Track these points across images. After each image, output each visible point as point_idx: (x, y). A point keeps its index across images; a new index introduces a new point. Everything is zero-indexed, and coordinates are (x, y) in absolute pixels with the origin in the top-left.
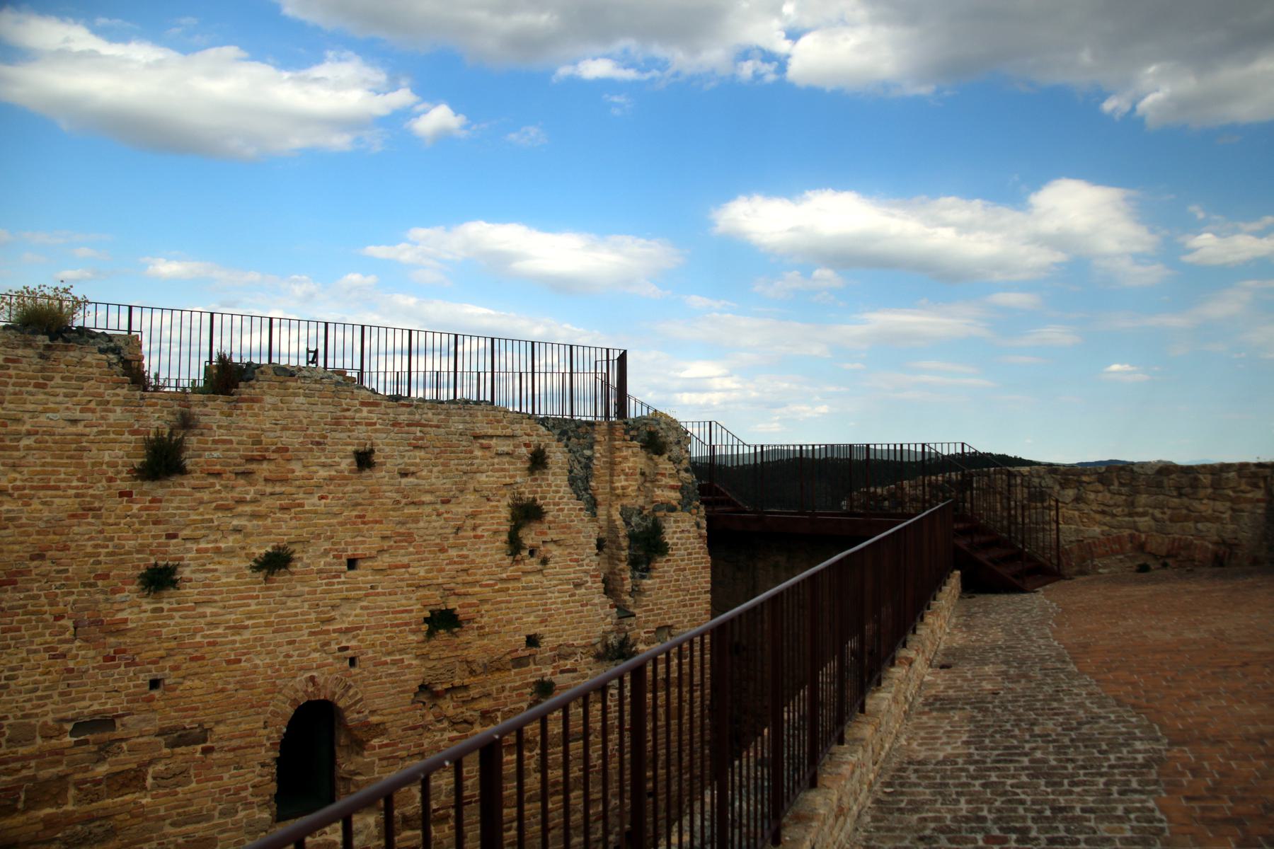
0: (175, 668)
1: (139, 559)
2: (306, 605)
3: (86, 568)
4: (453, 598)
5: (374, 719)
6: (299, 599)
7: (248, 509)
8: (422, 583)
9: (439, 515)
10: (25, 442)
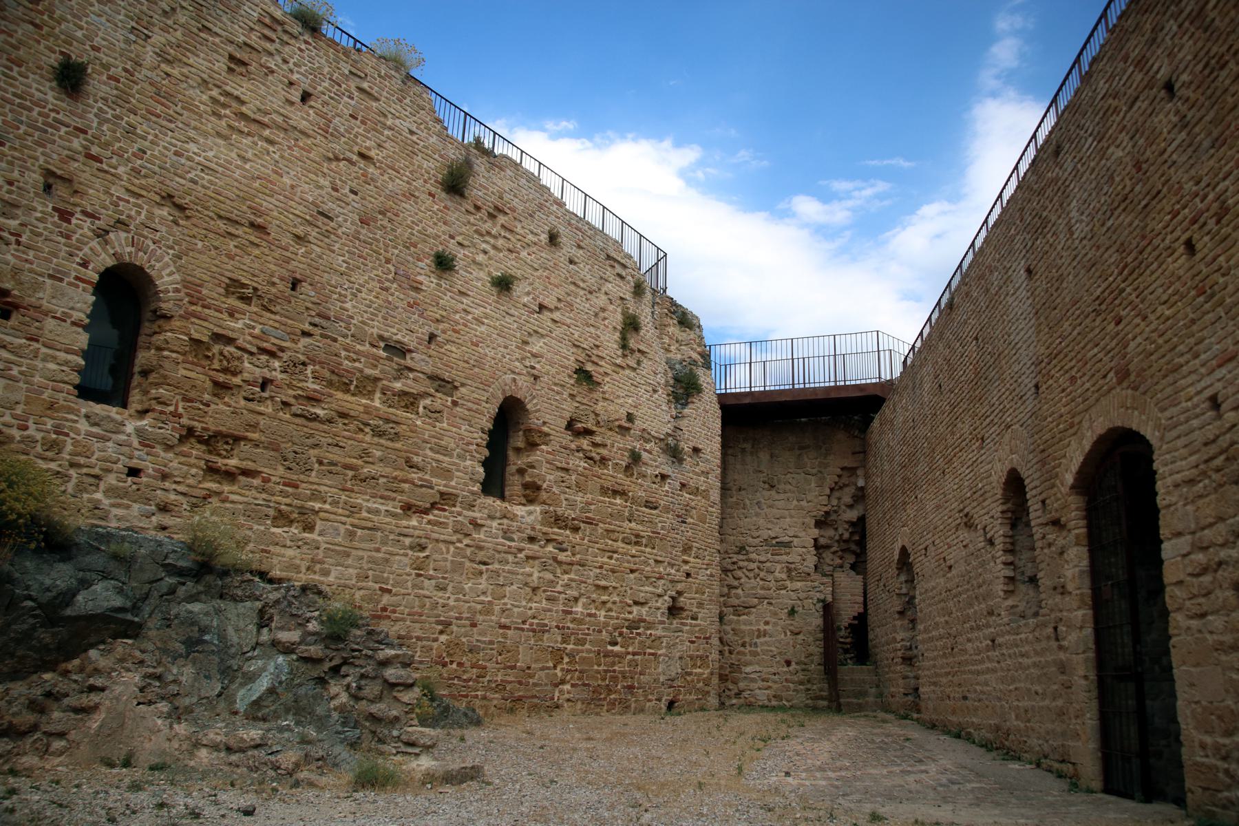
0: (444, 332)
1: (434, 245)
2: (516, 325)
3: (407, 235)
4: (590, 364)
5: (545, 429)
6: (513, 319)
7: (492, 241)
8: (576, 343)
9: (587, 299)
10: (386, 132)
